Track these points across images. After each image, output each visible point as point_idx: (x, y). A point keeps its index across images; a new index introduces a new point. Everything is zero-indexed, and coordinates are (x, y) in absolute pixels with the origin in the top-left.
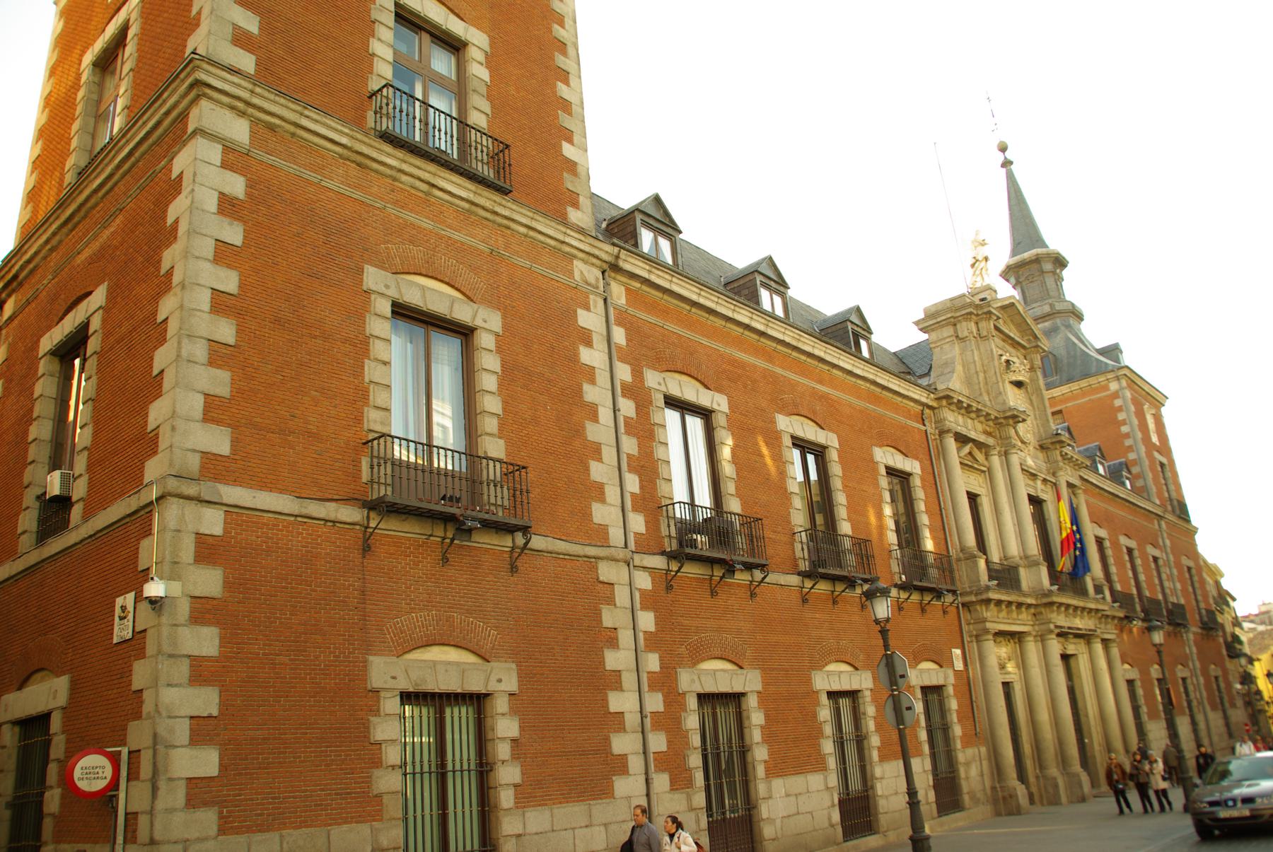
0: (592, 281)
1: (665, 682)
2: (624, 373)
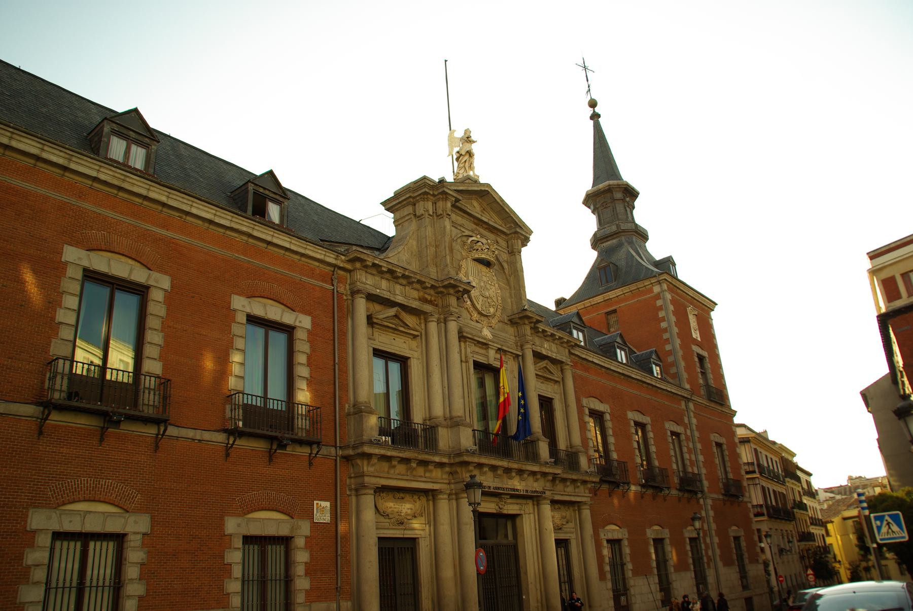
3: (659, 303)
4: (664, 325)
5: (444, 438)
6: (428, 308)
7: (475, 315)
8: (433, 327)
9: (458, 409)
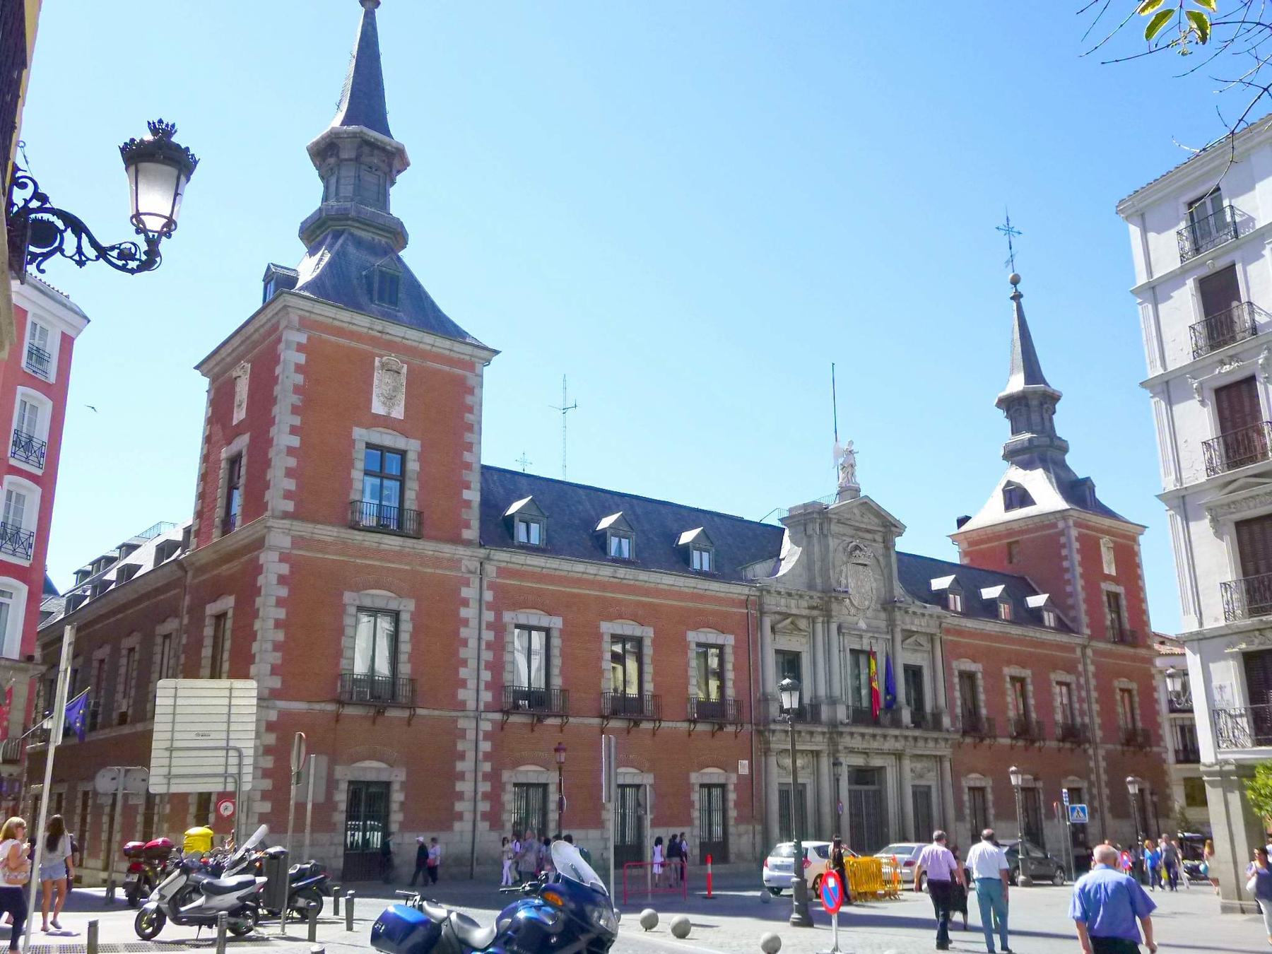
0: (472, 568)
1: (494, 777)
2: (489, 616)
6: (815, 613)
7: (853, 611)
8: (819, 627)
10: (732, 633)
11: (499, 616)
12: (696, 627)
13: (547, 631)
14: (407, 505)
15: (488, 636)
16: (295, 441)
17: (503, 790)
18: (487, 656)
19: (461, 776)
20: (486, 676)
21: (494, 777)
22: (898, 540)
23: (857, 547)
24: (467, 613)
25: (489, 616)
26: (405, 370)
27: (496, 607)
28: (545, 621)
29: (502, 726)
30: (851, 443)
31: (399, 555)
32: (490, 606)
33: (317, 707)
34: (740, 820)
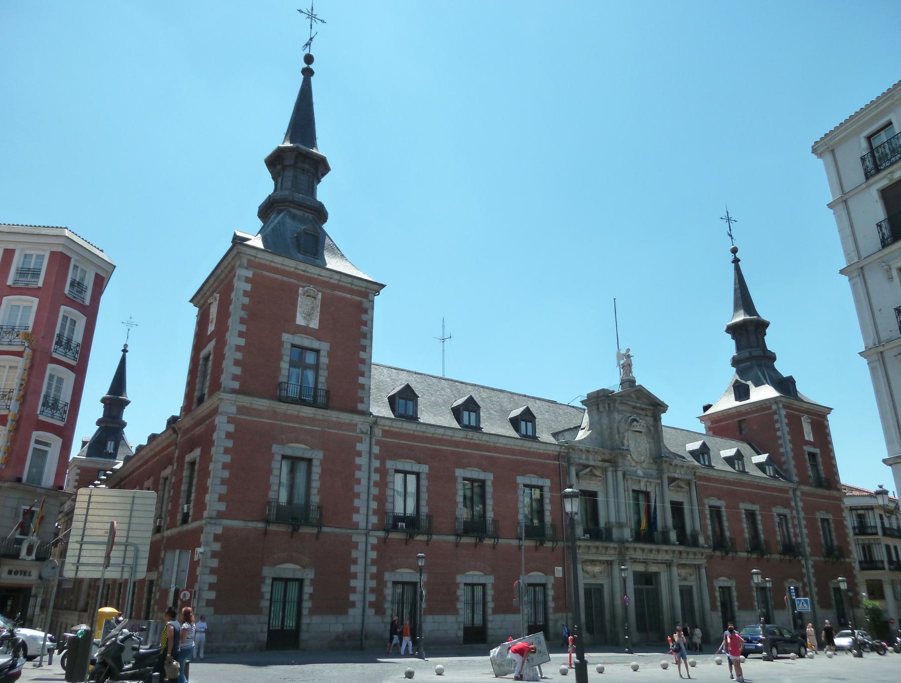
2: (376, 463)
3: (776, 417)
4: (779, 434)
5: (615, 533)
6: (607, 464)
7: (633, 464)
8: (610, 474)
9: (623, 519)
10: (547, 477)
11: (383, 463)
12: (523, 474)
13: (418, 475)
14: (320, 386)
15: (376, 477)
16: (242, 342)
17: (385, 586)
18: (375, 491)
19: (355, 576)
20: (374, 505)
21: (378, 577)
22: (663, 415)
23: (634, 420)
24: (362, 461)
25: (376, 463)
26: (320, 296)
27: (382, 458)
28: (416, 468)
29: (385, 540)
30: (628, 350)
31: (312, 421)
32: (377, 457)
33: (252, 525)
34: (557, 610)
